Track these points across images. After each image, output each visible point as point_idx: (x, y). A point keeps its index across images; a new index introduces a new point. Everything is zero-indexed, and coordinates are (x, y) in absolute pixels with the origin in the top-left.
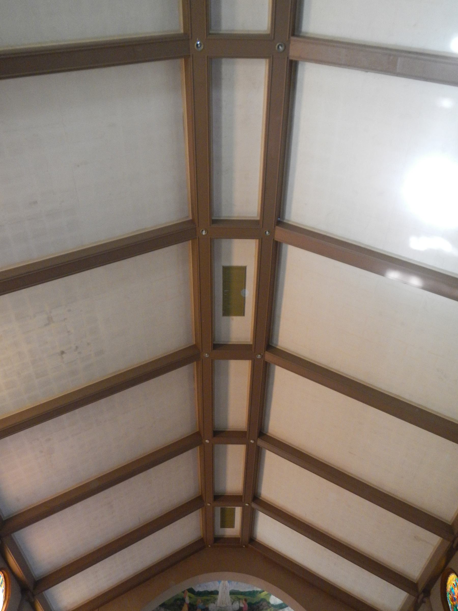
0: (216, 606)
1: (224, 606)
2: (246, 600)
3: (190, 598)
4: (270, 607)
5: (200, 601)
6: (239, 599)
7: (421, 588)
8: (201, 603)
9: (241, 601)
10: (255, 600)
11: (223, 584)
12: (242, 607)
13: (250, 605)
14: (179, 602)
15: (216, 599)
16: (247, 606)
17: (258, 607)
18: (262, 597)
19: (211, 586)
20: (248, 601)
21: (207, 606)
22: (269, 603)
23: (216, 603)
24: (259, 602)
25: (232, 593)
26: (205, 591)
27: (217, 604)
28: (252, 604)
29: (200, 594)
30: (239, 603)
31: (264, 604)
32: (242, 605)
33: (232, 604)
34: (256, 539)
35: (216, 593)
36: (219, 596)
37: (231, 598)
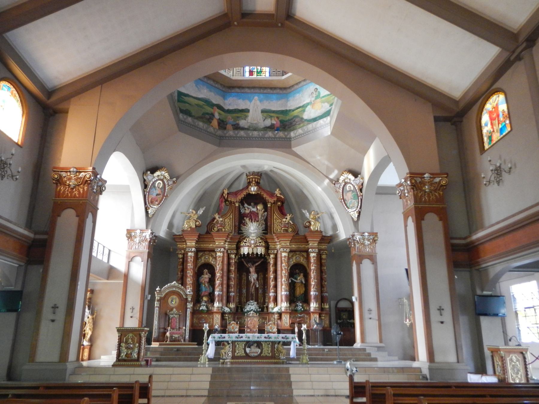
0: (248, 123)
1: (255, 122)
2: (278, 118)
3: (219, 114)
4: (304, 122)
5: (231, 118)
6: (271, 117)
7: (522, 38)
8: (231, 119)
9: (273, 118)
10: (288, 118)
11: (254, 104)
12: (274, 124)
13: (282, 122)
14: (208, 116)
15: (246, 117)
16: (279, 122)
17: (291, 123)
18: (296, 114)
19: (241, 104)
20: (280, 119)
21: (237, 122)
22: (302, 118)
23: (247, 120)
24: (292, 119)
25: (263, 111)
26: (235, 109)
27: (248, 121)
28: (284, 121)
29: (229, 111)
30: (271, 120)
31: (297, 120)
32: (274, 122)
33: (264, 120)
34: (295, 15)
35: (247, 111)
36: (250, 114)
37: (262, 115)
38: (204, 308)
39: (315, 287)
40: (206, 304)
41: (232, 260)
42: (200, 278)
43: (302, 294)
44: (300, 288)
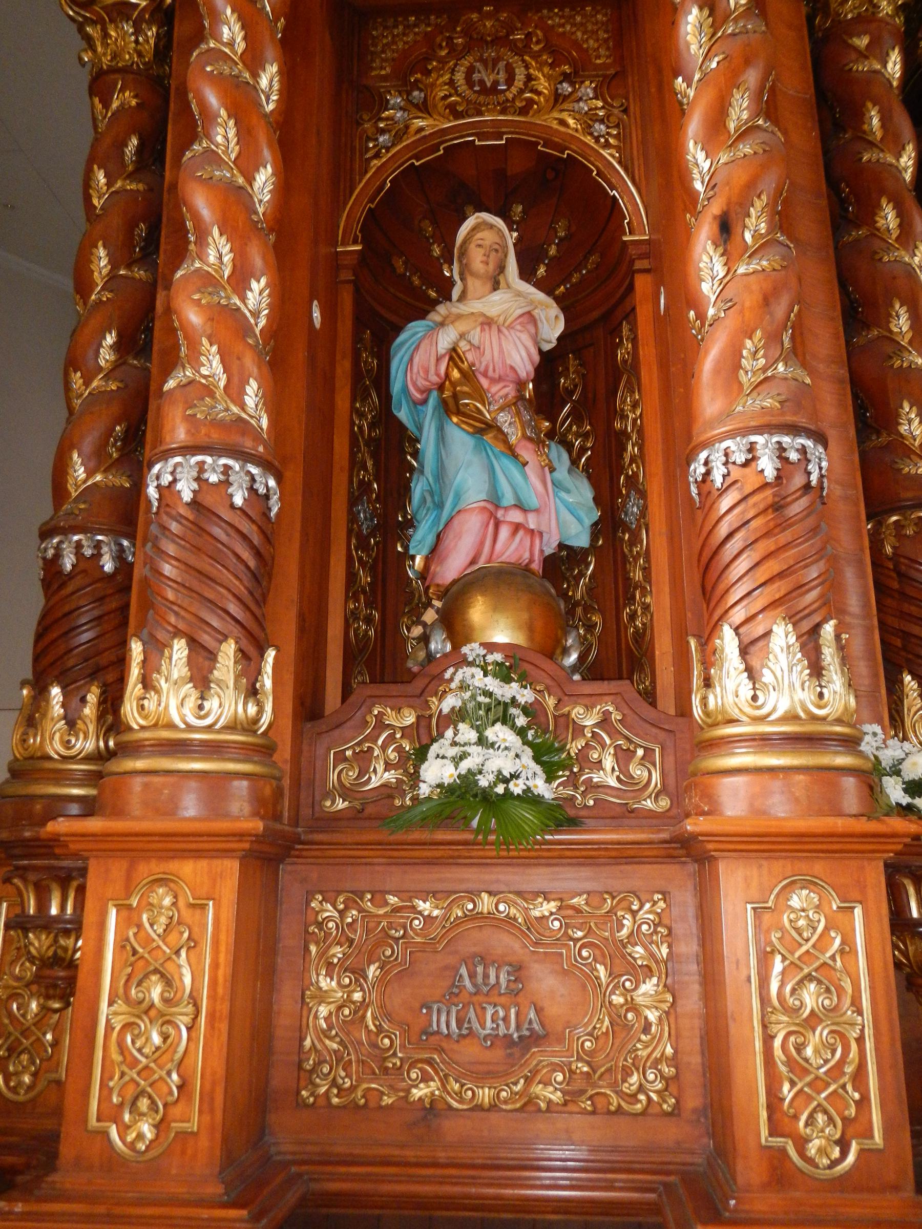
38: (502, 763)
40: (526, 696)
41: (878, 51)
42: (416, 328)
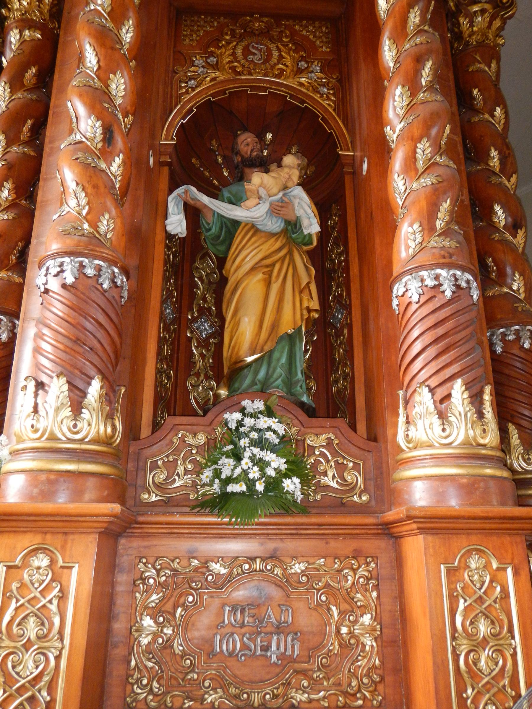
39: (439, 224)
43: (291, 339)
44: (268, 284)
